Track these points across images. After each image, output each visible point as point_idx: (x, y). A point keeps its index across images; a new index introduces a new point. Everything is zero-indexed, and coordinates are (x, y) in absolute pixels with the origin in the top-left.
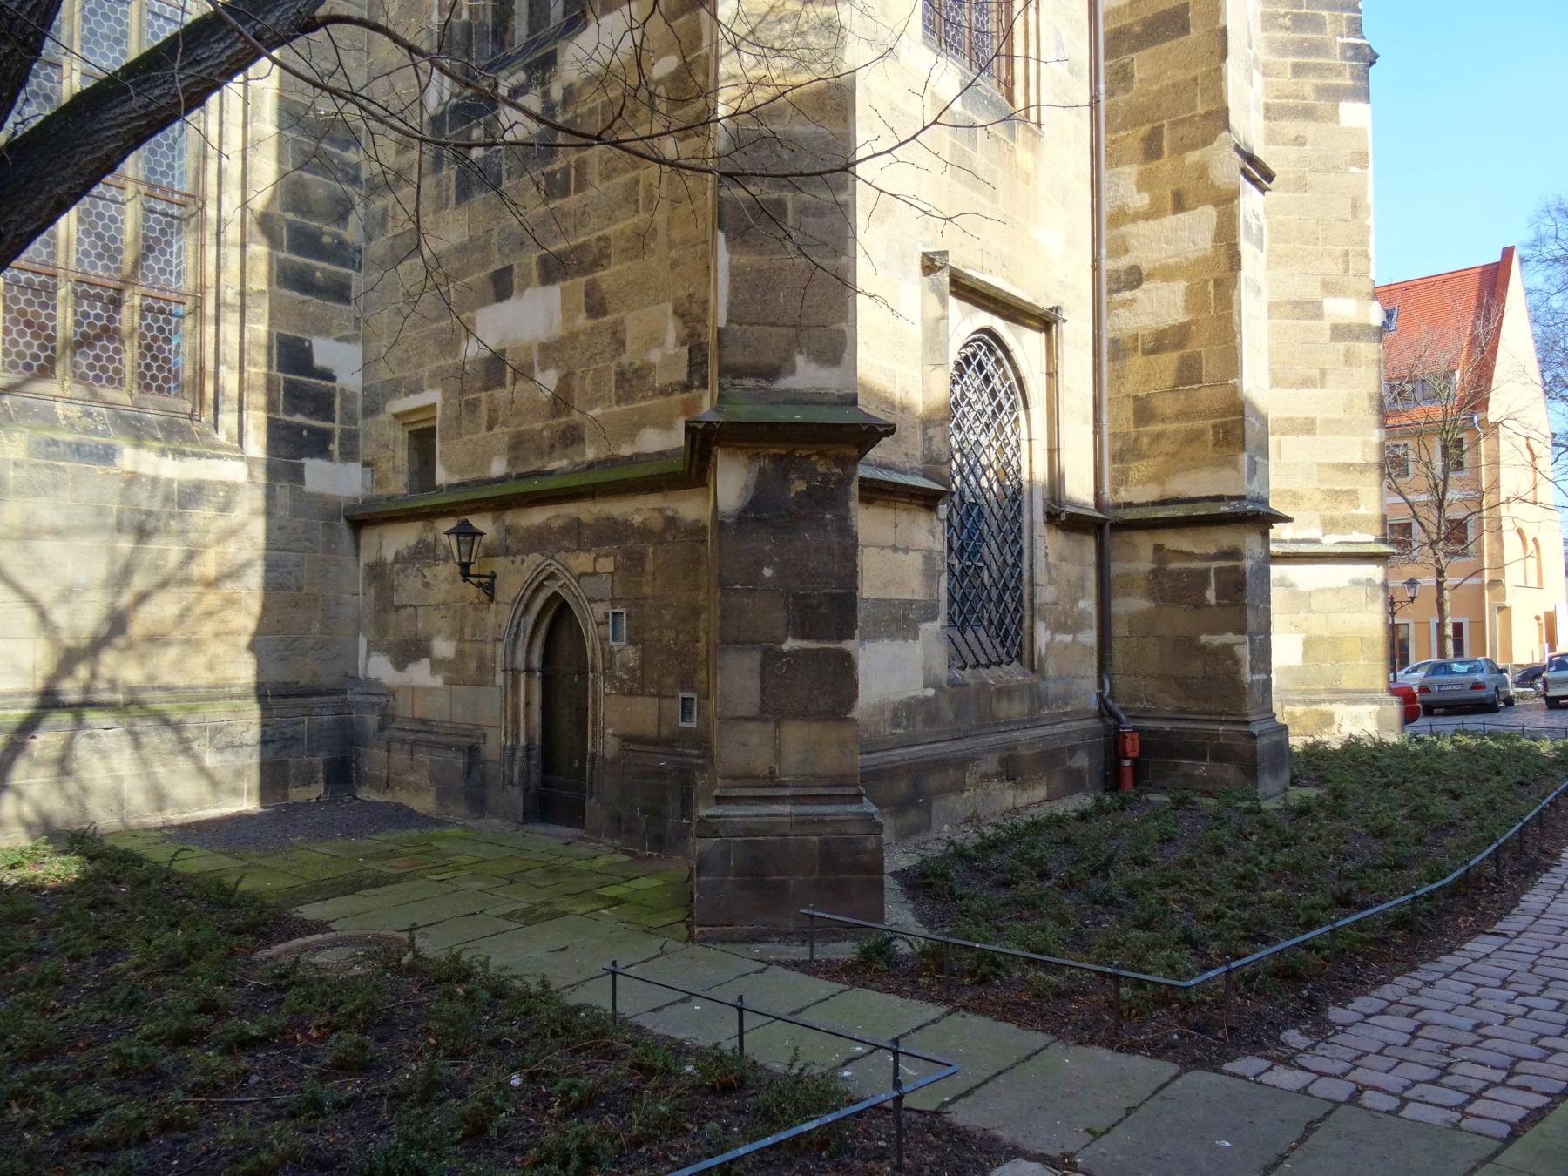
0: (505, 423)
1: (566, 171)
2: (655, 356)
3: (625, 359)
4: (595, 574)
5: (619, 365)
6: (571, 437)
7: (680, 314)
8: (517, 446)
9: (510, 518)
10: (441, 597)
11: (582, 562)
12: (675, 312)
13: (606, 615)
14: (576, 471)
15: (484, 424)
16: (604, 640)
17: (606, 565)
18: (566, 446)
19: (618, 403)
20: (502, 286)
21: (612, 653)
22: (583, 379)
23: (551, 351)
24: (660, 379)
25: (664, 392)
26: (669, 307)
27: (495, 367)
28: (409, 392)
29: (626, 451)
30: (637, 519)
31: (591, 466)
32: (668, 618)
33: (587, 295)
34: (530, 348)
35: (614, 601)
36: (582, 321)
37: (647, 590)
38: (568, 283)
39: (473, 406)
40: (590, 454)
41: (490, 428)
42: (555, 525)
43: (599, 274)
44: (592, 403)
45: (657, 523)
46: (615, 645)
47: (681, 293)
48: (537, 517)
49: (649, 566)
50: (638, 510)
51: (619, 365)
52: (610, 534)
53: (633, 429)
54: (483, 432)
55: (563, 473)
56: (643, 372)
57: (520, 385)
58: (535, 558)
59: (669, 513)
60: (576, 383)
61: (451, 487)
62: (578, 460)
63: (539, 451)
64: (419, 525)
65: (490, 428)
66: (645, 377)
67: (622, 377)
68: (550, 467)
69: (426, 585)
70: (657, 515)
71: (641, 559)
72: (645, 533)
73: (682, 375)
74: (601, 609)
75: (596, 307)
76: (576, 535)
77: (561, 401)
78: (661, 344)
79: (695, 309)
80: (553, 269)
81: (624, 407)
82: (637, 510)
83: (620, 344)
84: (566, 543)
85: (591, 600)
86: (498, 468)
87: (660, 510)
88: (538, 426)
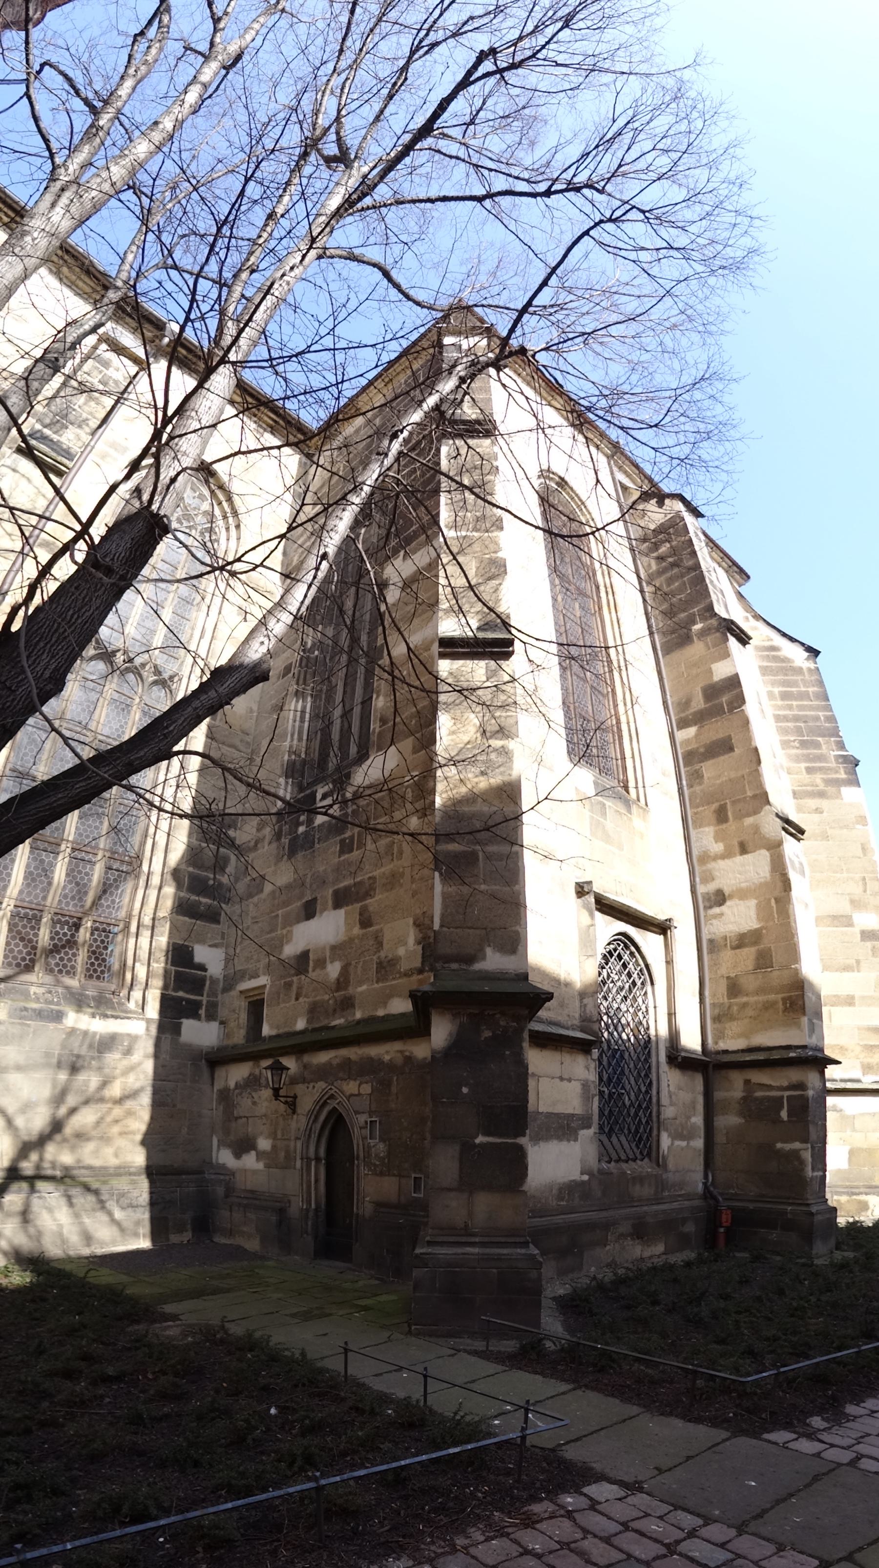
0: (306, 996)
2: (401, 951)
3: (382, 954)
4: (359, 1095)
5: (379, 958)
6: (347, 1004)
7: (417, 925)
8: (313, 1011)
9: (306, 1058)
11: (351, 1087)
12: (414, 923)
13: (366, 1122)
15: (294, 997)
16: (364, 1138)
17: (366, 1089)
18: (343, 1010)
19: (377, 982)
20: (309, 911)
21: (369, 1147)
22: (356, 967)
23: (337, 950)
24: (404, 966)
25: (407, 974)
26: (411, 921)
27: (303, 960)
28: (251, 978)
29: (381, 1013)
31: (359, 1022)
32: (405, 1124)
33: (361, 914)
34: (324, 948)
36: (357, 931)
38: (350, 908)
39: (288, 985)
40: (358, 1015)
41: (297, 999)
42: (335, 1062)
43: (369, 901)
44: (360, 983)
45: (399, 1060)
46: (372, 1142)
47: (418, 911)
48: (323, 1057)
49: (394, 1089)
50: (387, 1052)
51: (379, 958)
54: (293, 1002)
56: (393, 962)
57: (318, 971)
58: (321, 1085)
59: (407, 1054)
60: (351, 969)
62: (350, 1019)
64: (250, 1064)
65: (297, 999)
66: (394, 965)
67: (380, 965)
68: (334, 1023)
69: (254, 1103)
70: (399, 1055)
72: (391, 1067)
73: (417, 963)
74: (362, 1118)
75: (365, 922)
76: (348, 1069)
77: (343, 982)
78: (406, 944)
79: (427, 921)
80: (340, 900)
81: (381, 985)
83: (379, 944)
84: (341, 1075)
85: (357, 1113)
87: (401, 1052)
88: (326, 997)
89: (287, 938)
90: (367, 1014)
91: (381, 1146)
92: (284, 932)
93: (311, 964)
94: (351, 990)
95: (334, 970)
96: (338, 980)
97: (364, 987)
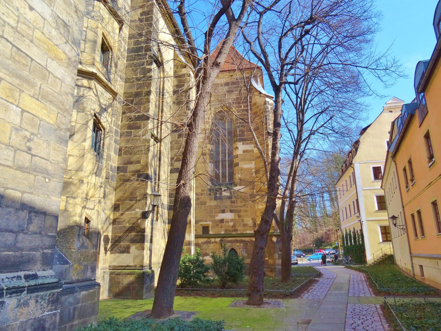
0: (224, 227)
1: (234, 201)
2: (249, 223)
3: (244, 223)
6: (236, 230)
7: (252, 219)
8: (226, 230)
9: (225, 239)
10: (212, 248)
11: (238, 244)
14: (236, 234)
15: (220, 227)
16: (242, 253)
17: (242, 245)
20: (223, 212)
23: (231, 220)
25: (250, 227)
26: (251, 219)
27: (222, 221)
28: (204, 222)
29: (245, 232)
30: (246, 240)
31: (239, 234)
34: (228, 220)
35: (243, 249)
36: (237, 218)
37: (248, 248)
39: (218, 225)
40: (239, 232)
41: (221, 228)
44: (239, 227)
45: (249, 240)
48: (230, 239)
49: (248, 245)
52: (241, 242)
53: (246, 230)
54: (220, 228)
55: (234, 234)
57: (226, 223)
58: (230, 244)
60: (236, 224)
61: (213, 234)
63: (230, 231)
64: (207, 239)
65: (221, 228)
67: (244, 225)
69: (209, 246)
71: (247, 244)
72: (248, 242)
73: (252, 225)
74: (241, 250)
75: (239, 216)
76: (237, 241)
77: (234, 226)
80: (231, 211)
82: (247, 239)
83: (243, 221)
86: (223, 233)
88: (230, 228)
89: (217, 216)
90: (241, 233)
91: (246, 254)
92: (215, 214)
93: (225, 222)
94: (236, 228)
95: (231, 224)
96: (233, 226)
97: (240, 228)
